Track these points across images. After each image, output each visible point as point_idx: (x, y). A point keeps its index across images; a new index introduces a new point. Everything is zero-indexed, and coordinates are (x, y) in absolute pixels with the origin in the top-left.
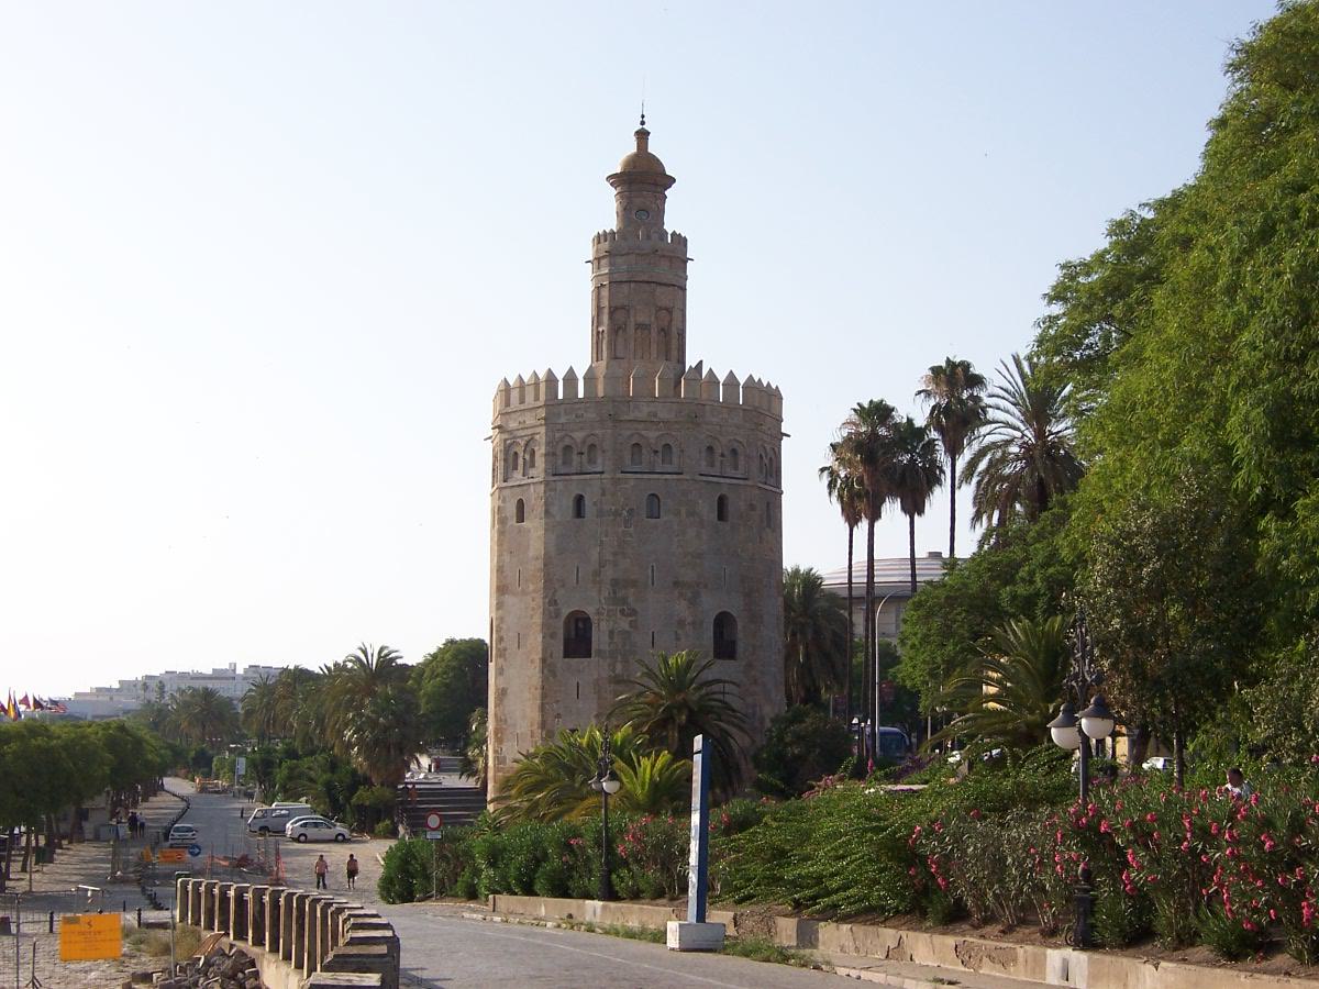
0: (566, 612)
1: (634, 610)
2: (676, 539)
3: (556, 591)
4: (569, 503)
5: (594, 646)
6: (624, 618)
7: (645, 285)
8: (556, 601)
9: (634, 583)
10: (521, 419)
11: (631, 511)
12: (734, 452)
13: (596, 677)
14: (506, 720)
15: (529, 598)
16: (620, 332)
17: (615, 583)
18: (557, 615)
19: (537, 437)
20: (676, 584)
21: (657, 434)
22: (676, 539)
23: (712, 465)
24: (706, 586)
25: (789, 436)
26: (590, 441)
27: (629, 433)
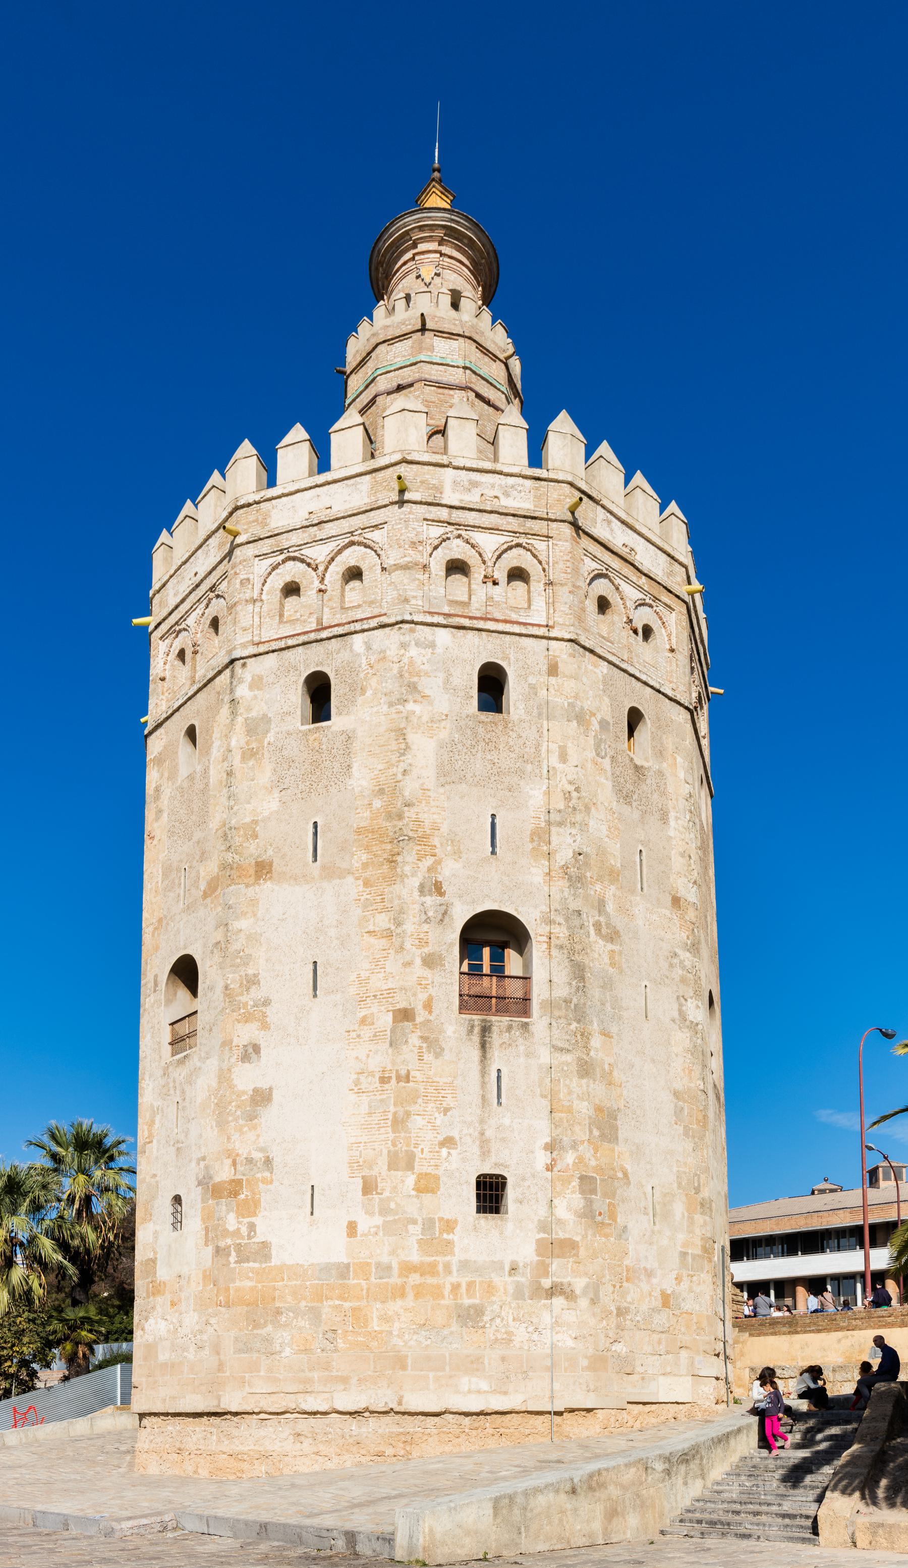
3: (439, 862)
5: (539, 993)
8: (438, 888)
14: (268, 1162)
15: (351, 887)
18: (445, 914)
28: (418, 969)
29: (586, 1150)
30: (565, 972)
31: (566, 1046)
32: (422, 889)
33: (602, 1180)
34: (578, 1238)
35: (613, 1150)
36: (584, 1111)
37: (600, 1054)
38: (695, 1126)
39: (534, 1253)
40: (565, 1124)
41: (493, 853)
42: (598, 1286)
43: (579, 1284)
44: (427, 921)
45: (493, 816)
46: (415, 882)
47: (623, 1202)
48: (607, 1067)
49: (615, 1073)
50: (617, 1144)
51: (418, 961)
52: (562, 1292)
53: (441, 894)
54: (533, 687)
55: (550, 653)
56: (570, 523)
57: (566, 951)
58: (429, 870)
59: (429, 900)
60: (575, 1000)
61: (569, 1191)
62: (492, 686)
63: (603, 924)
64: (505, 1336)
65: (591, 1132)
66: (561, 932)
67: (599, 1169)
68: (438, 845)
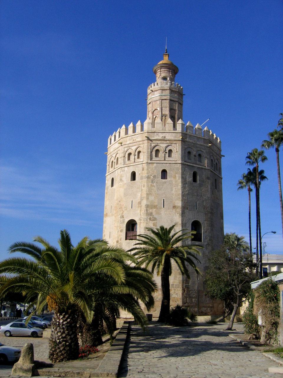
0: (127, 221)
2: (174, 188)
3: (123, 212)
4: (129, 176)
7: (166, 101)
8: (123, 216)
9: (155, 207)
10: (114, 147)
11: (154, 177)
12: (200, 155)
16: (156, 118)
17: (147, 206)
18: (124, 222)
19: (119, 152)
20: (174, 207)
21: (167, 145)
22: (174, 188)
23: (189, 159)
25: (224, 156)
26: (138, 150)
27: (153, 145)
28: (120, 233)
32: (121, 218)
41: (132, 208)
44: (121, 223)
45: (132, 201)
46: (120, 216)
51: (119, 231)
53: (123, 218)
54: (140, 174)
58: (122, 213)
59: (121, 219)
63: (152, 218)
68: (123, 208)
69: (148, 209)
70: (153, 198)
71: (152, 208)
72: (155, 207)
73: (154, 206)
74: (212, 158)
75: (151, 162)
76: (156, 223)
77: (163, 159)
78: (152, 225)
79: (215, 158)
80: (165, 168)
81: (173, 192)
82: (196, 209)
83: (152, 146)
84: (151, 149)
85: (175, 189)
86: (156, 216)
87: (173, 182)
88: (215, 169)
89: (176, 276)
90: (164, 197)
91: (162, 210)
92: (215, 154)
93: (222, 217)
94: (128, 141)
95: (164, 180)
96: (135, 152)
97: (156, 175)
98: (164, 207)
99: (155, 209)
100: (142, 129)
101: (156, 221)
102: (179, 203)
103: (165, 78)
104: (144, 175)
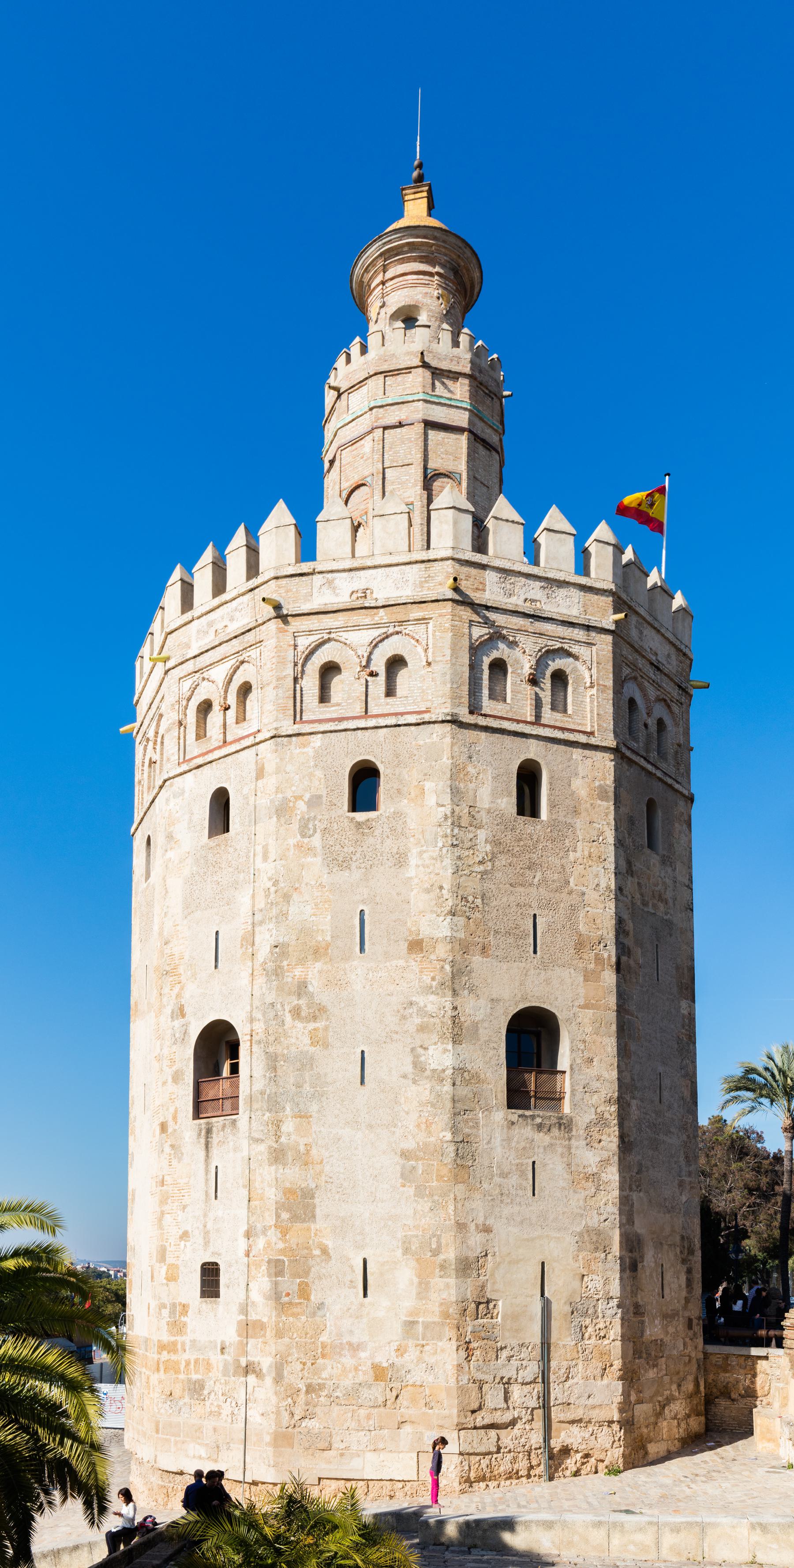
1: (322, 1009)
6: (299, 1025)
13: (245, 1154)
20: (416, 946)
24: (484, 950)
29: (273, 1235)
30: (261, 1066)
31: (261, 1137)
33: (290, 1261)
34: (265, 1320)
35: (309, 1229)
36: (273, 1197)
37: (293, 1137)
38: (435, 1184)
39: (236, 1335)
40: (259, 1212)
42: (282, 1365)
43: (266, 1363)
47: (320, 1278)
48: (302, 1148)
49: (314, 1152)
50: (314, 1222)
52: (254, 1372)
55: (259, 757)
56: (276, 618)
57: (262, 1045)
60: (268, 1092)
61: (260, 1275)
62: (221, 802)
63: (304, 1007)
64: (216, 1409)
65: (278, 1216)
66: (259, 1027)
67: (282, 1251)
69: (285, 963)
70: (309, 909)
71: (302, 961)
72: (318, 952)
73: (316, 952)
74: (631, 690)
75: (296, 728)
76: (326, 1029)
77: (359, 709)
78: (309, 1042)
79: (652, 693)
80: (369, 753)
81: (411, 872)
82: (535, 952)
83: (300, 648)
84: (296, 665)
85: (421, 853)
86: (324, 998)
87: (409, 821)
88: (647, 751)
89: (428, 1283)
90: (363, 902)
91: (355, 963)
92: (651, 673)
93: (687, 988)
94: (195, 637)
95: (361, 816)
96: (226, 692)
97: (324, 793)
98: (362, 949)
99: (318, 965)
100: (253, 569)
101: (327, 1019)
102: (439, 928)
103: (408, 318)
104: (263, 801)
